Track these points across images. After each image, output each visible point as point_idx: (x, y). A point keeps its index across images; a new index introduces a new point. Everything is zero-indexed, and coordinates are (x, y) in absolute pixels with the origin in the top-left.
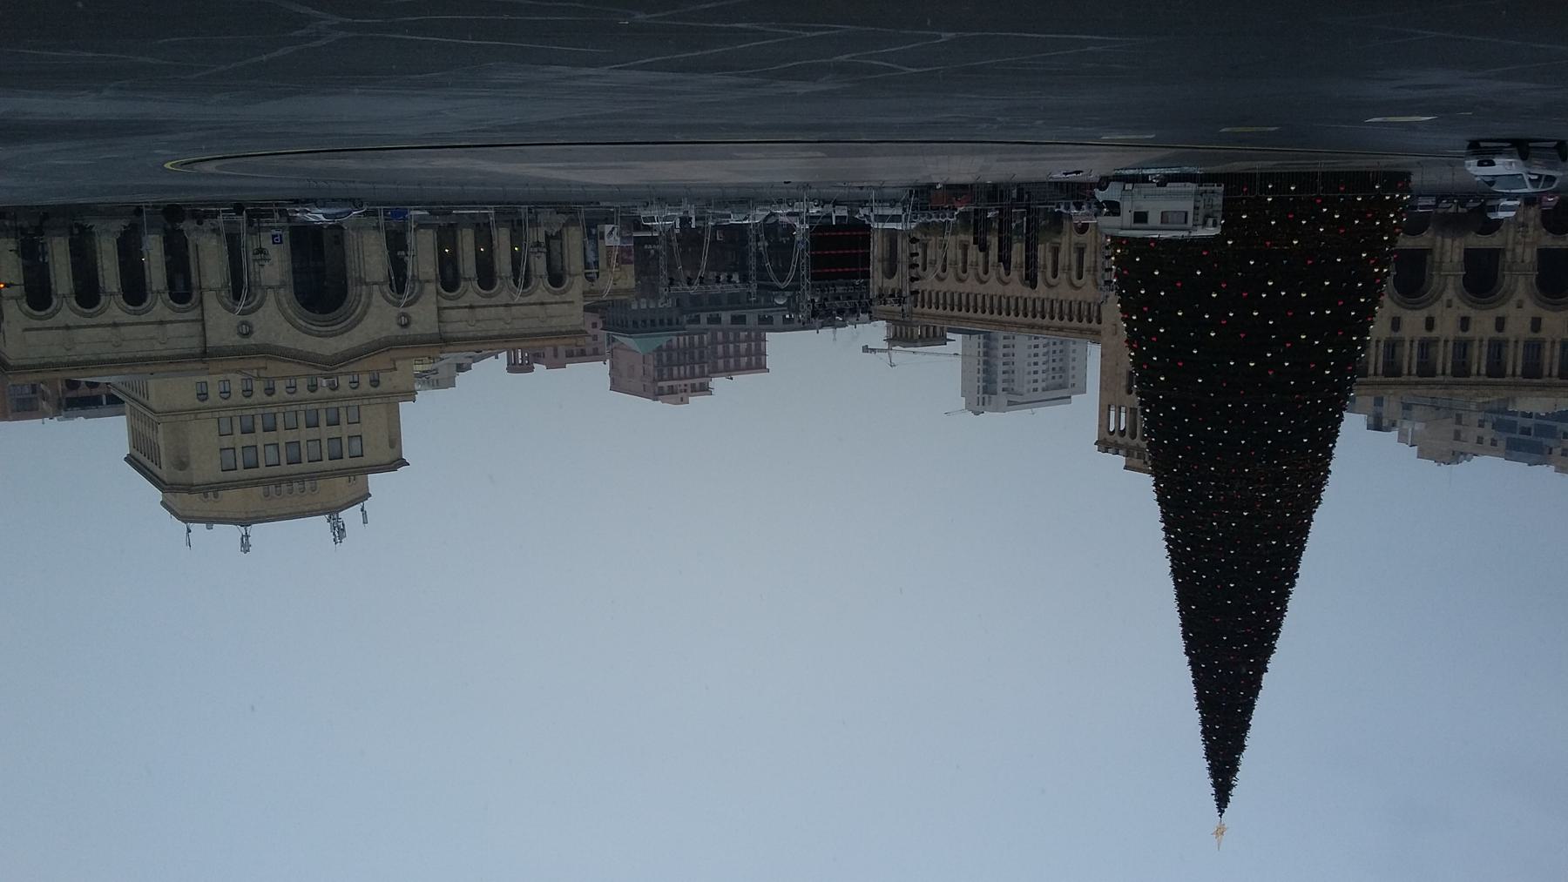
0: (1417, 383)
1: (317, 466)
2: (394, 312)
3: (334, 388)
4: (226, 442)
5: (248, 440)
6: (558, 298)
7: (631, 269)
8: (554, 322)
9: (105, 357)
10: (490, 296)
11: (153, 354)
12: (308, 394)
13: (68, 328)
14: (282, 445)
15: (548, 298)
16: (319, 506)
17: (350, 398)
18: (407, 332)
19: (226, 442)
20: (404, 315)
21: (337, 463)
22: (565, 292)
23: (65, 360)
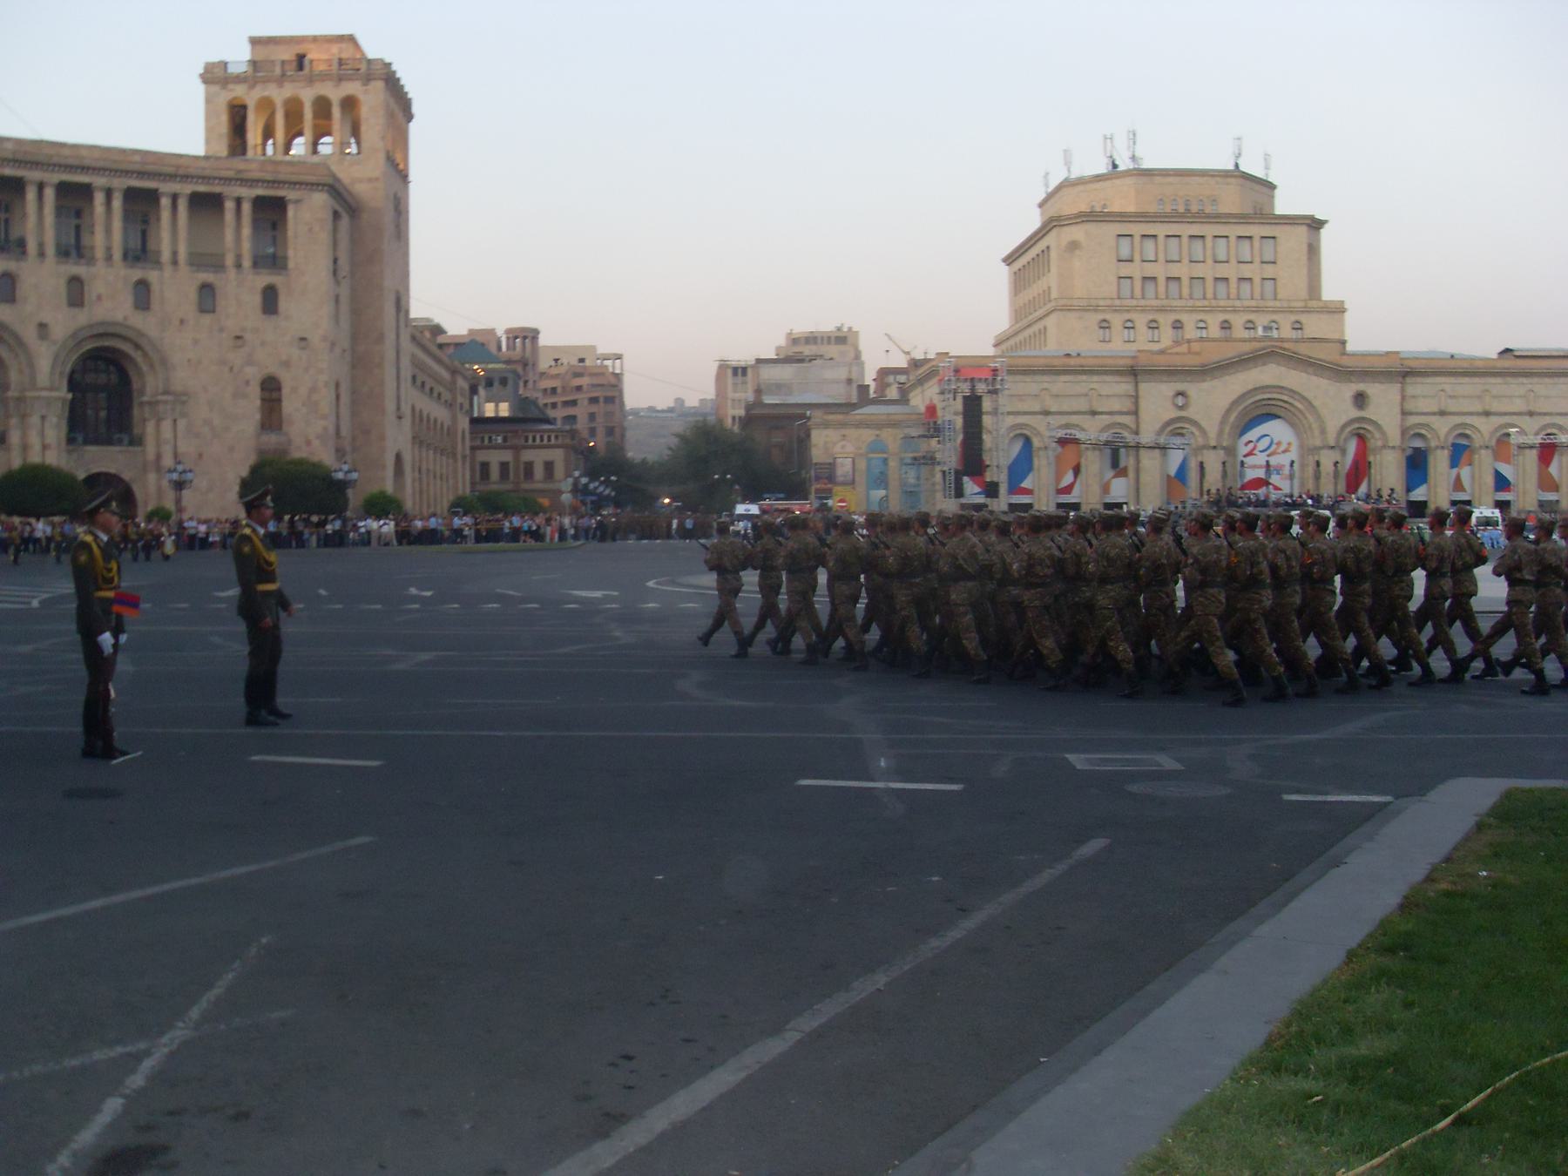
4: (1269, 271)
7: (817, 455)
9: (1499, 380)
10: (1067, 426)
11: (1452, 380)
12: (1184, 317)
13: (1531, 414)
16: (1158, 179)
18: (1180, 387)
19: (1269, 271)
20: (1181, 408)
23: (1536, 380)
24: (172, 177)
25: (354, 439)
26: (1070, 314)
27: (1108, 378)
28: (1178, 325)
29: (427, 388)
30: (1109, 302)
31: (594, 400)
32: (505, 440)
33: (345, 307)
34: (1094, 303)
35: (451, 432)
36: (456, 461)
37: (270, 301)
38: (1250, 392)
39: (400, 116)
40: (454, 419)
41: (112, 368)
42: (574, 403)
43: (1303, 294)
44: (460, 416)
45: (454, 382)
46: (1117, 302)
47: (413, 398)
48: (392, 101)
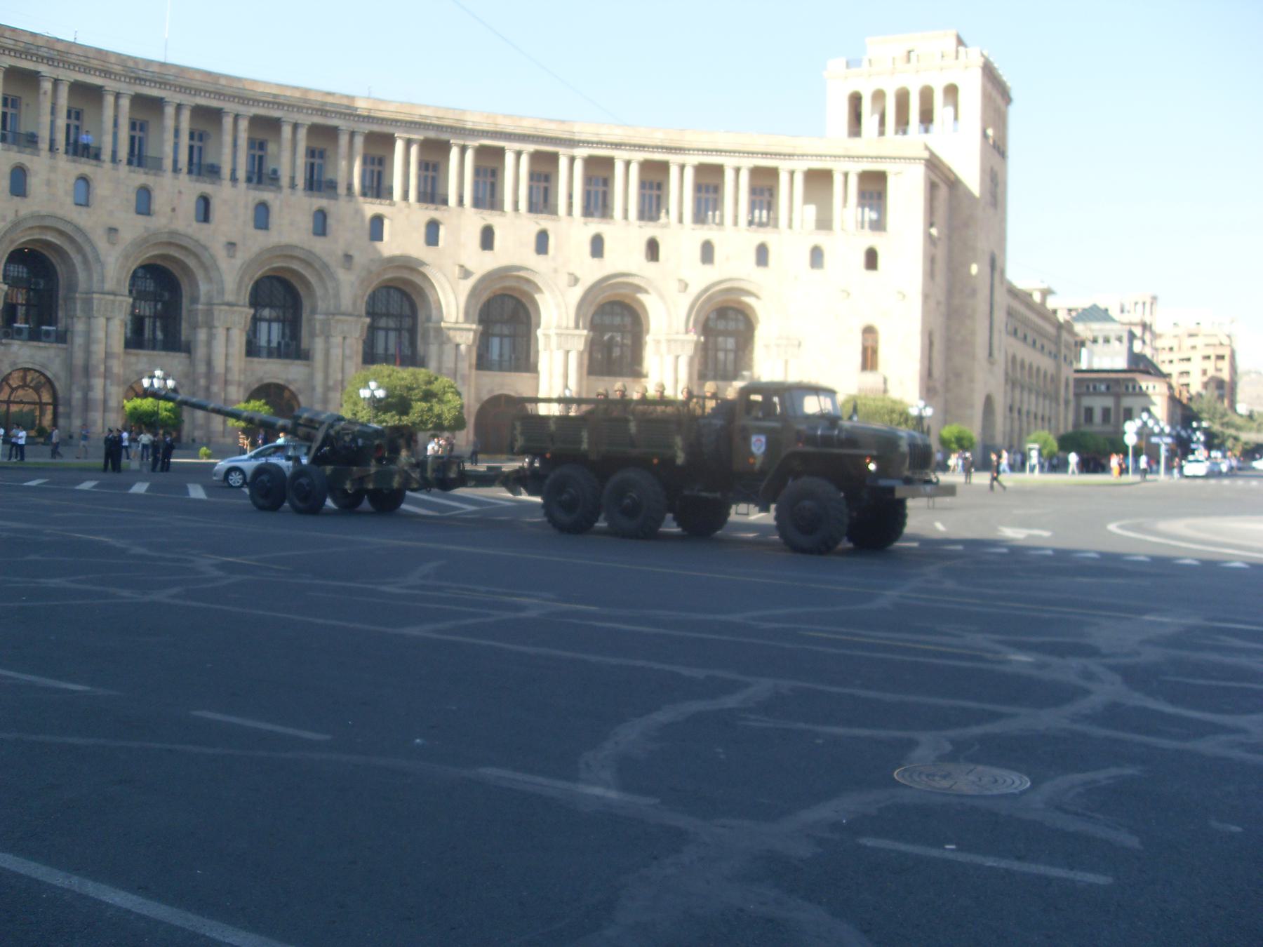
0: (617, 146)
24: (790, 156)
25: (947, 381)
29: (1029, 340)
31: (1208, 357)
32: (1108, 388)
33: (940, 265)
35: (1055, 379)
36: (1058, 404)
37: (871, 259)
39: (999, 100)
40: (1058, 368)
41: (740, 317)
42: (1189, 360)
44: (1063, 365)
45: (1059, 336)
47: (1006, 345)
48: (989, 86)
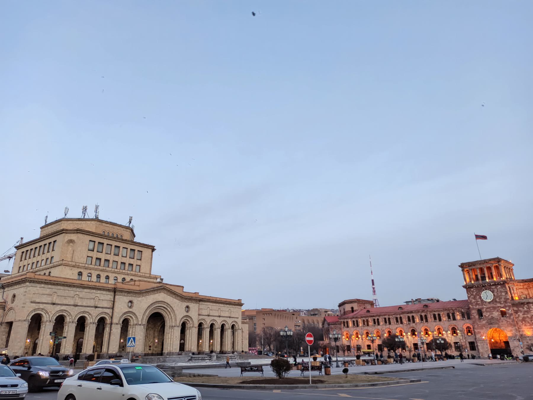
1: (110, 242)
2: (133, 310)
3: (99, 276)
4: (139, 262)
5: (132, 261)
6: (41, 306)
8: (48, 291)
9: (223, 305)
10: (84, 312)
12: (110, 275)
13: (230, 317)
14: (120, 256)
15: (49, 307)
16: (104, 224)
17: (93, 269)
18: (131, 298)
19: (139, 262)
20: (130, 307)
21: (102, 240)
22: (35, 310)
26: (67, 267)
27: (104, 292)
28: (107, 277)
30: (84, 265)
34: (78, 264)
38: (154, 303)
43: (148, 272)
46: (87, 266)
